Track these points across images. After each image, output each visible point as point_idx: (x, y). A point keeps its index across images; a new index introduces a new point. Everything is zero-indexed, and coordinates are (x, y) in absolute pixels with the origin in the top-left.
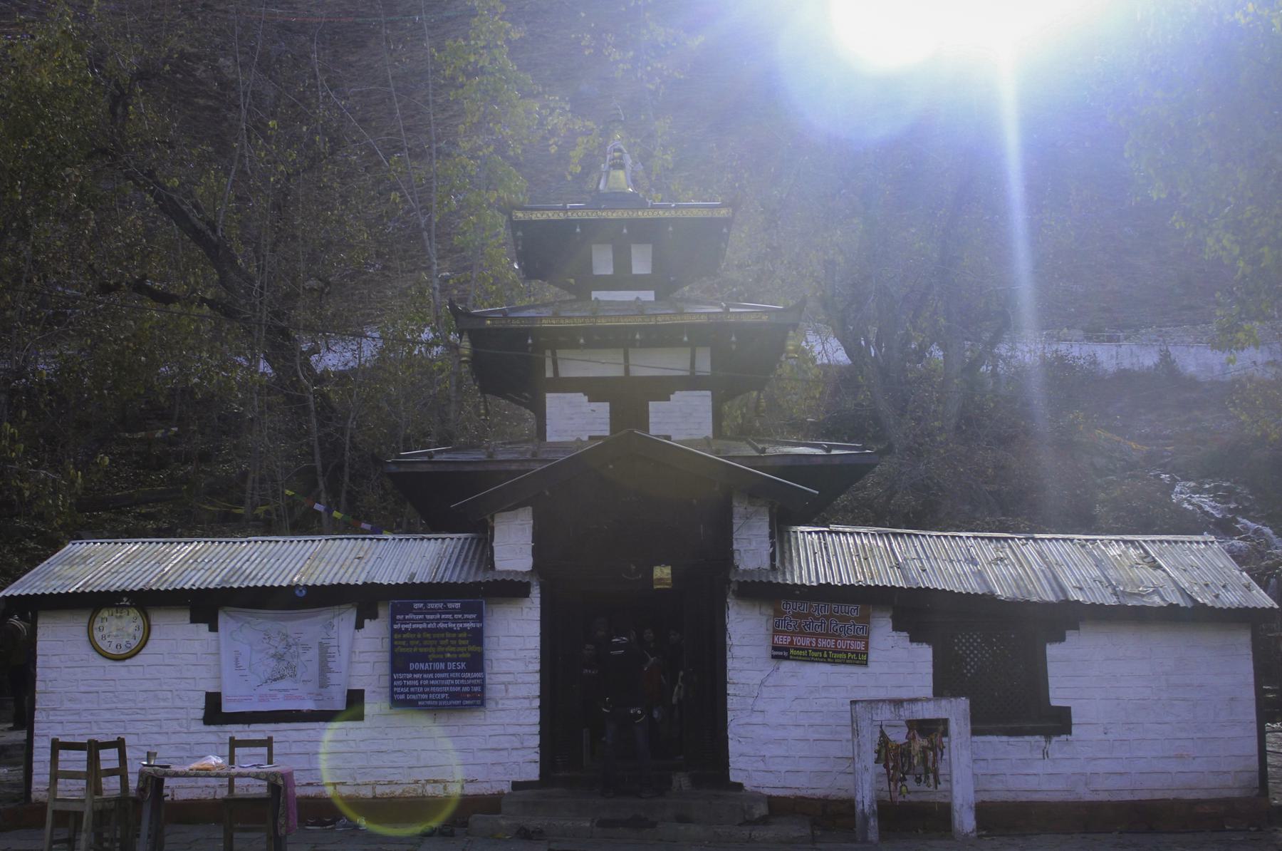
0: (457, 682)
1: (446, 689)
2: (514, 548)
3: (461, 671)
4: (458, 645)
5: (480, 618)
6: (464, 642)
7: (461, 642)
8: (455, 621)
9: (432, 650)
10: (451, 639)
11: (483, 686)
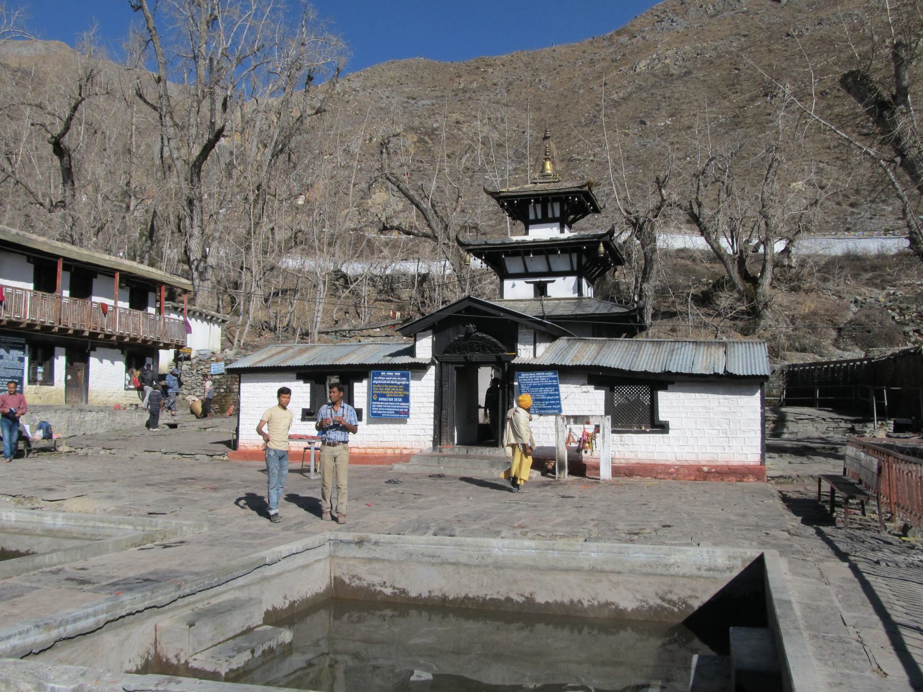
2: (424, 348)
5: (408, 380)
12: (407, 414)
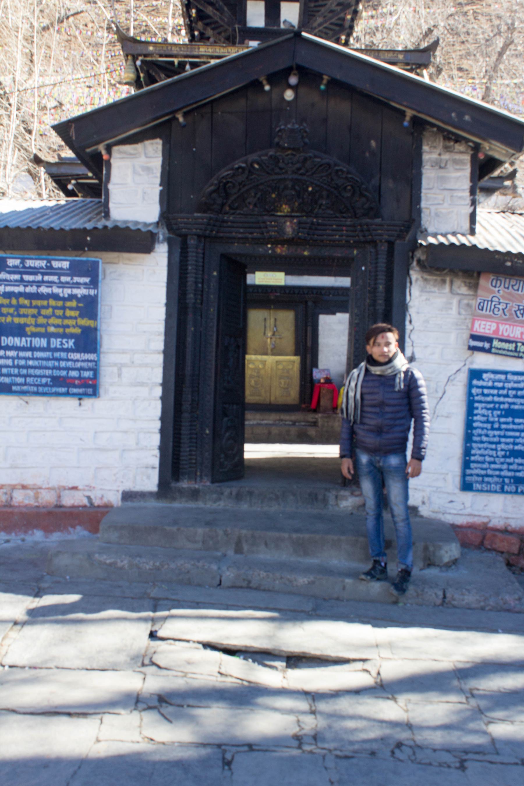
0: (63, 364)
1: (48, 372)
3: (67, 350)
4: (64, 317)
5: (94, 283)
6: (73, 313)
7: (68, 313)
8: (62, 285)
9: (30, 321)
10: (55, 308)
11: (96, 371)
12: (88, 386)
